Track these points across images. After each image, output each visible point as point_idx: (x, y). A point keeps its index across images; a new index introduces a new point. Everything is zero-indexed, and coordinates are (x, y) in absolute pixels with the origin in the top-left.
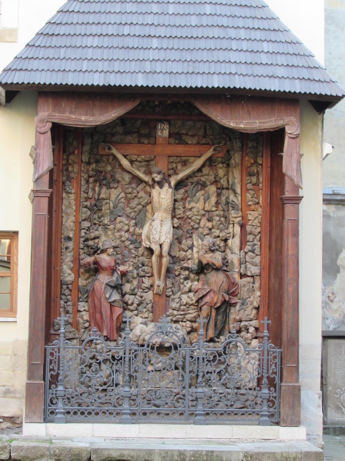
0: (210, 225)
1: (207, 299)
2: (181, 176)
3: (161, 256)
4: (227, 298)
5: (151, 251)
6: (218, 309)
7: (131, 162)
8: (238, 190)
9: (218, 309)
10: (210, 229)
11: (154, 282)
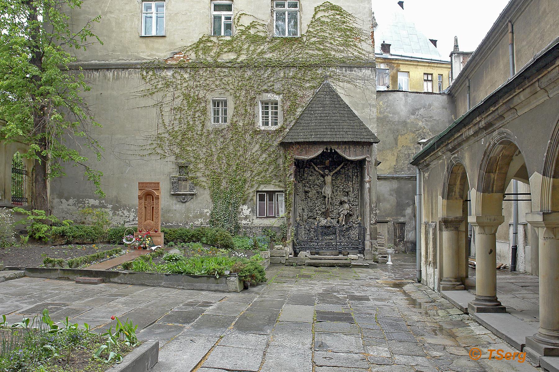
0: (343, 188)
1: (343, 212)
2: (334, 172)
3: (328, 198)
4: (349, 212)
5: (325, 197)
6: (346, 215)
7: (318, 168)
8: (351, 177)
9: (346, 215)
10: (343, 189)
11: (326, 206)
